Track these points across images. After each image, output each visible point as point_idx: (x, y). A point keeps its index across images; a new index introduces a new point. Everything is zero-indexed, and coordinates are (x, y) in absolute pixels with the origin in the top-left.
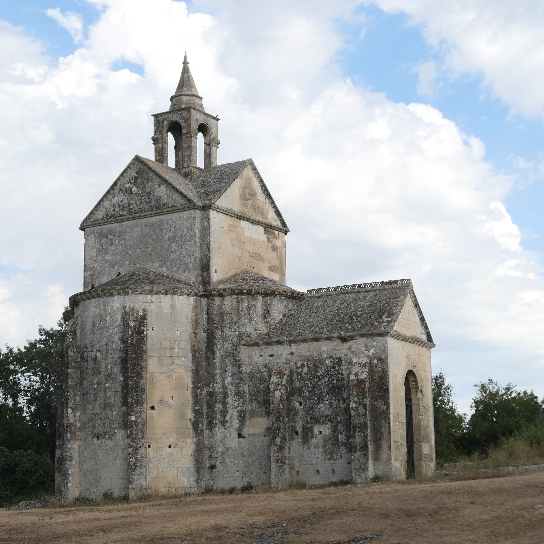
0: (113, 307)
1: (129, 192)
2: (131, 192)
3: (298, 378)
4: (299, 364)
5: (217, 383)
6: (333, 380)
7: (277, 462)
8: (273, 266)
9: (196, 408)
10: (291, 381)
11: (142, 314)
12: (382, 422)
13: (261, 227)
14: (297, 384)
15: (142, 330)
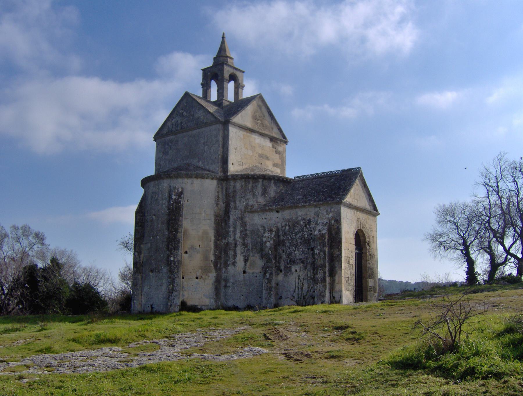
0: (163, 186)
1: (182, 115)
3: (282, 234)
4: (284, 224)
6: (305, 235)
7: (267, 290)
8: (276, 164)
10: (278, 235)
11: (181, 191)
13: (268, 138)
14: (282, 238)
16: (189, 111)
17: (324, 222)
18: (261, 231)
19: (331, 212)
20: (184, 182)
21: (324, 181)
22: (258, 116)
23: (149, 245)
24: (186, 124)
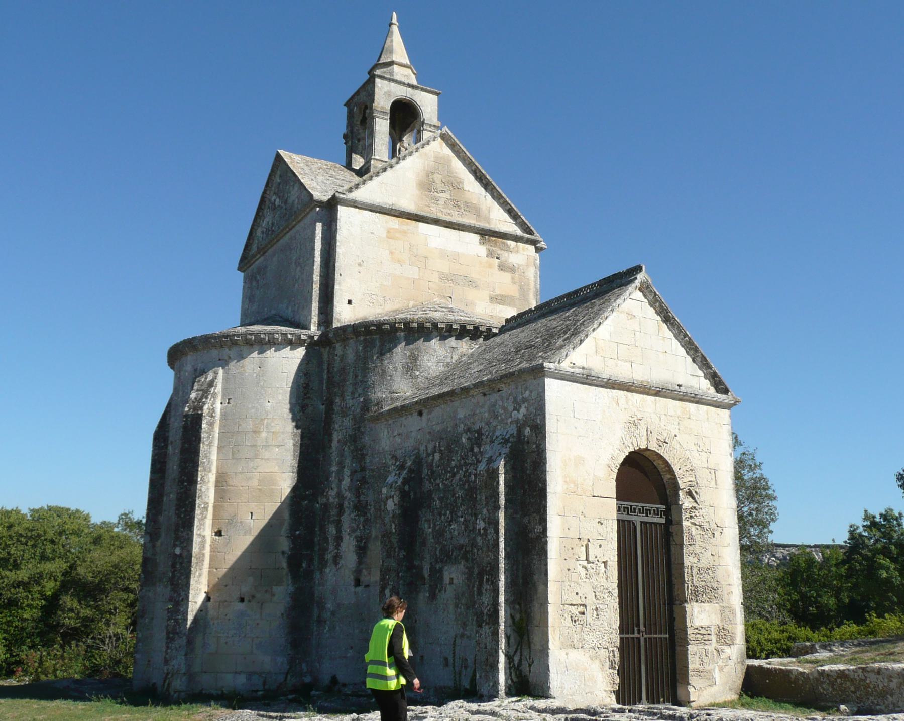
8: (502, 296)
9: (297, 532)
12: (534, 561)
20: (221, 358)
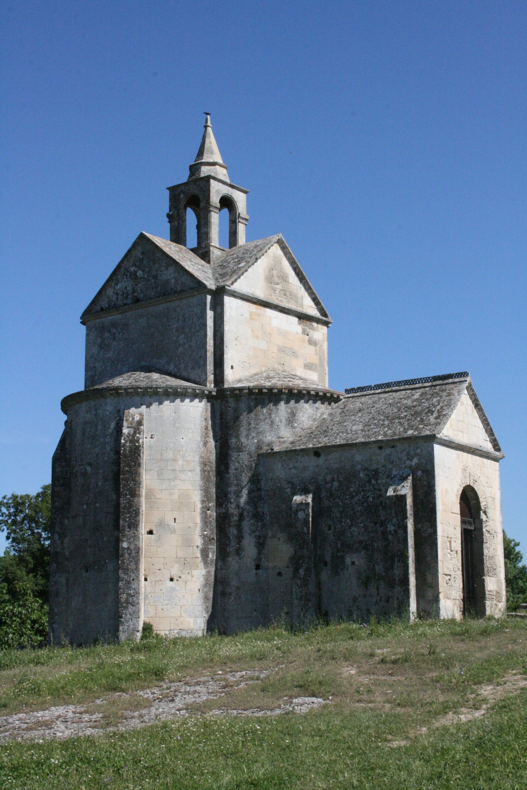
1: (134, 276)
2: (136, 277)
4: (328, 478)
5: (231, 502)
6: (368, 497)
7: (300, 599)
8: (310, 364)
11: (138, 419)
15: (138, 437)
16: (147, 269)
17: (403, 473)
18: (287, 490)
19: (416, 455)
21: (401, 397)
22: (275, 276)
23: (81, 519)
24: (142, 293)
